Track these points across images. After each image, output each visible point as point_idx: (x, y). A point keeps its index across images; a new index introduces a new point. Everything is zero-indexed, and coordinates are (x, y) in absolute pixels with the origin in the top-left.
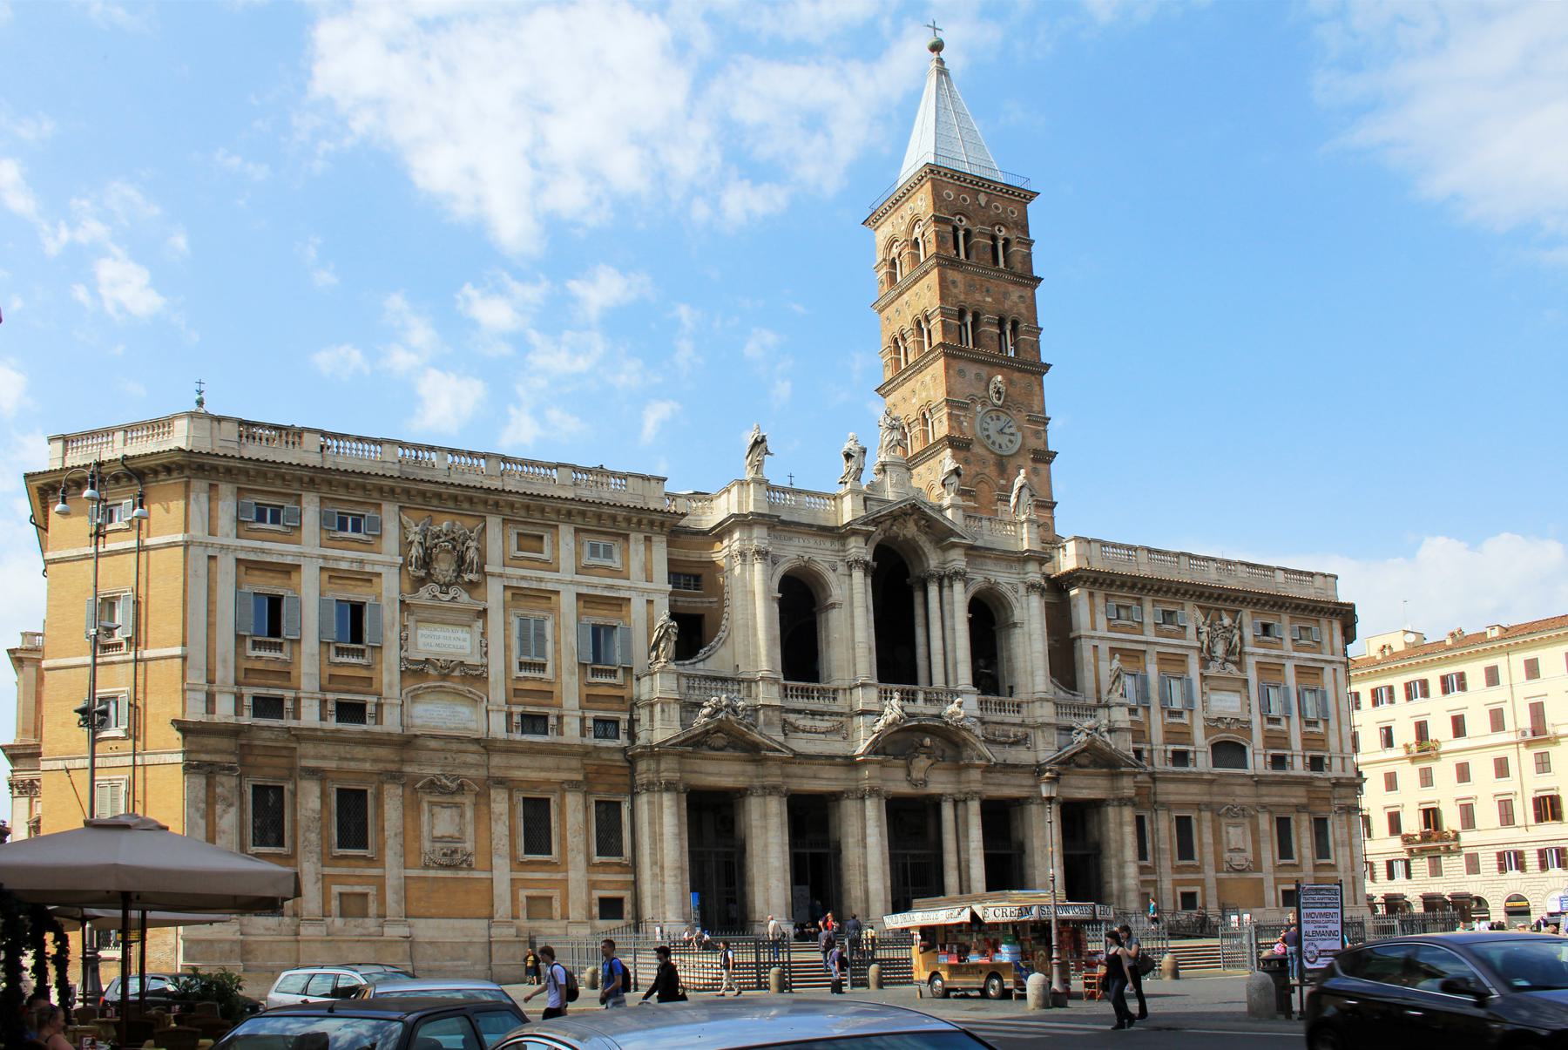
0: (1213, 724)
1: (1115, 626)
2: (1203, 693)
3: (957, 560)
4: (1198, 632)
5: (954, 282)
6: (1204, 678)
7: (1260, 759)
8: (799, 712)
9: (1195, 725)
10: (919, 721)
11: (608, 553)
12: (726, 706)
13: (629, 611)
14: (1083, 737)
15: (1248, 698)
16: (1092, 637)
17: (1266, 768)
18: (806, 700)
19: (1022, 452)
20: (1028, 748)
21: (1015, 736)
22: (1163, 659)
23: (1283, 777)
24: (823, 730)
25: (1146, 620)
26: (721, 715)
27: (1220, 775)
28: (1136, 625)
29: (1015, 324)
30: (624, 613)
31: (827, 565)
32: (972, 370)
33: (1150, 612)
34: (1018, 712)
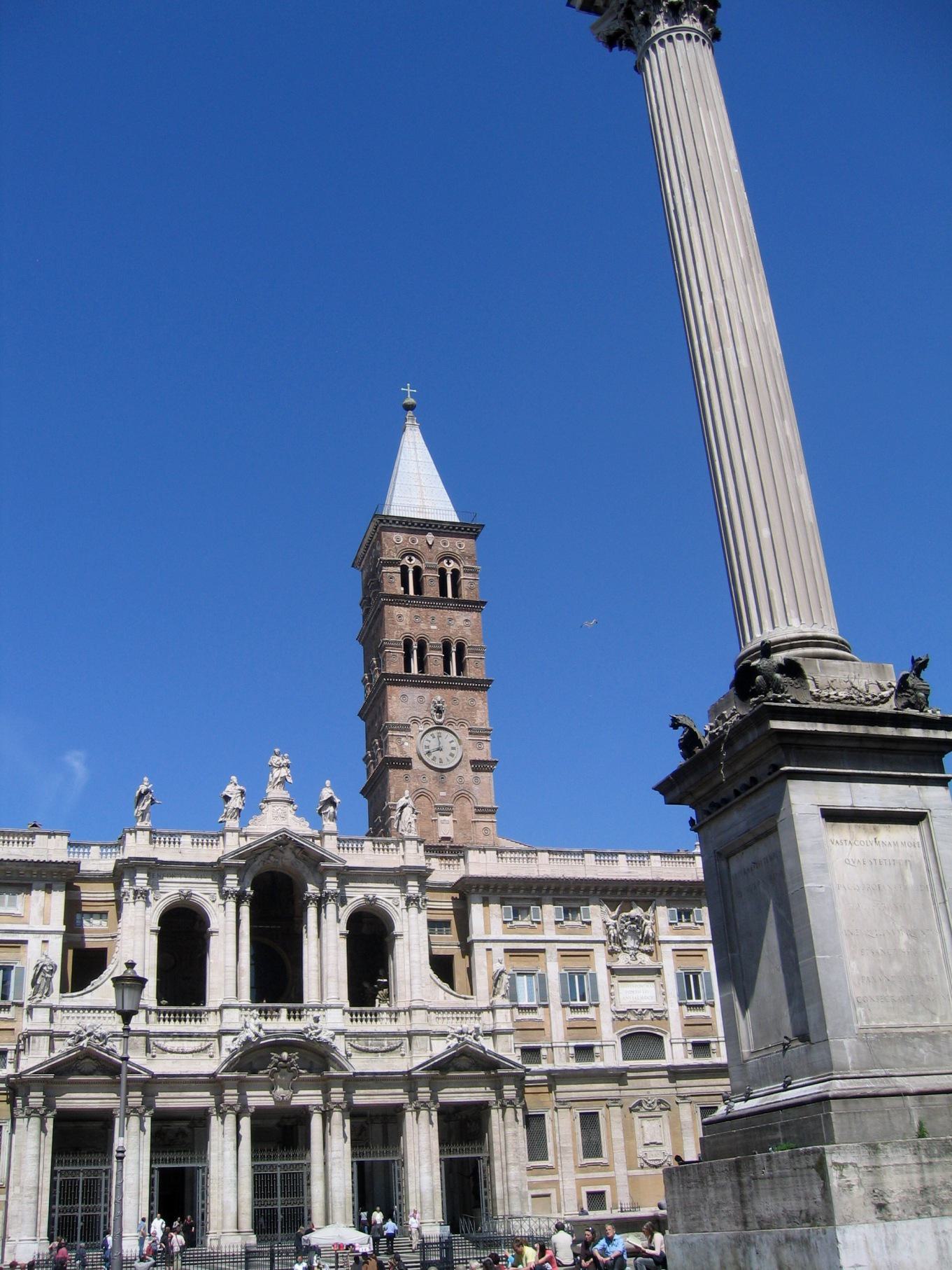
0: (620, 1016)
3: (332, 885)
6: (613, 971)
7: (679, 1049)
9: (602, 1018)
10: (276, 1037)
11: (13, 904)
12: (89, 1035)
13: (26, 952)
14: (454, 1042)
16: (485, 941)
17: (686, 1057)
18: (177, 1021)
19: (463, 763)
20: (403, 1055)
22: (565, 954)
23: (703, 1066)
24: (190, 1049)
25: (545, 919)
26: (84, 1043)
27: (628, 1070)
28: (535, 925)
29: (461, 648)
30: (22, 953)
31: (206, 897)
32: (414, 693)
33: (549, 912)
34: (396, 1020)
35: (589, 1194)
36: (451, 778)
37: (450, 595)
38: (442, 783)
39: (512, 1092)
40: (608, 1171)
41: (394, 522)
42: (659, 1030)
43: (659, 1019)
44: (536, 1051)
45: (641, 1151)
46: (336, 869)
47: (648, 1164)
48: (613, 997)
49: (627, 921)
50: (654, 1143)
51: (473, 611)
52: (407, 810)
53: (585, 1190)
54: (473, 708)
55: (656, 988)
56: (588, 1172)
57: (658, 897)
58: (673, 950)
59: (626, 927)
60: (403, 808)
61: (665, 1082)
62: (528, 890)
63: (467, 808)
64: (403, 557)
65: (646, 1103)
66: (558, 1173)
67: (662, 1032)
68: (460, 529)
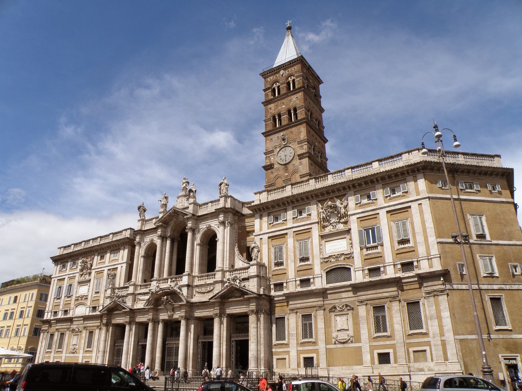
1: (273, 226)
2: (321, 245)
4: (319, 214)
5: (270, 108)
8: (140, 294)
10: (163, 290)
11: (116, 256)
15: (350, 239)
16: (259, 235)
21: (209, 289)
22: (297, 233)
32: (275, 137)
33: (290, 214)
35: (305, 359)
36: (290, 167)
37: (292, 89)
38: (286, 170)
39: (253, 306)
40: (316, 345)
41: (267, 73)
42: (348, 265)
43: (349, 258)
44: (282, 284)
45: (334, 335)
46: (190, 218)
47: (338, 341)
48: (321, 251)
49: (329, 208)
50: (344, 329)
51: (299, 92)
52: (223, 185)
53: (302, 356)
54: (300, 133)
55: (347, 241)
56: (305, 346)
57: (348, 191)
58: (358, 218)
59: (329, 212)
60: (221, 184)
61: (351, 294)
62: (279, 205)
63: (298, 176)
64: (273, 85)
65: (339, 307)
66: (289, 347)
67: (350, 265)
68: (293, 63)
